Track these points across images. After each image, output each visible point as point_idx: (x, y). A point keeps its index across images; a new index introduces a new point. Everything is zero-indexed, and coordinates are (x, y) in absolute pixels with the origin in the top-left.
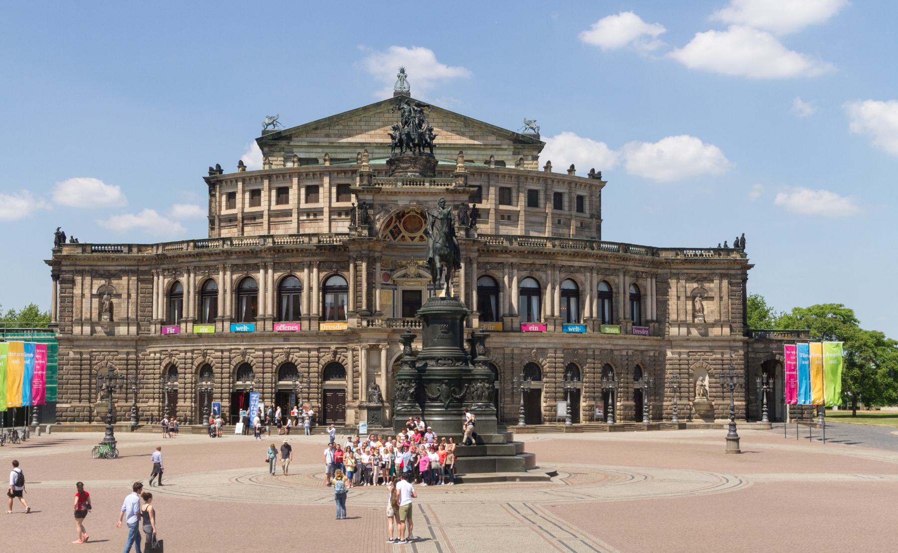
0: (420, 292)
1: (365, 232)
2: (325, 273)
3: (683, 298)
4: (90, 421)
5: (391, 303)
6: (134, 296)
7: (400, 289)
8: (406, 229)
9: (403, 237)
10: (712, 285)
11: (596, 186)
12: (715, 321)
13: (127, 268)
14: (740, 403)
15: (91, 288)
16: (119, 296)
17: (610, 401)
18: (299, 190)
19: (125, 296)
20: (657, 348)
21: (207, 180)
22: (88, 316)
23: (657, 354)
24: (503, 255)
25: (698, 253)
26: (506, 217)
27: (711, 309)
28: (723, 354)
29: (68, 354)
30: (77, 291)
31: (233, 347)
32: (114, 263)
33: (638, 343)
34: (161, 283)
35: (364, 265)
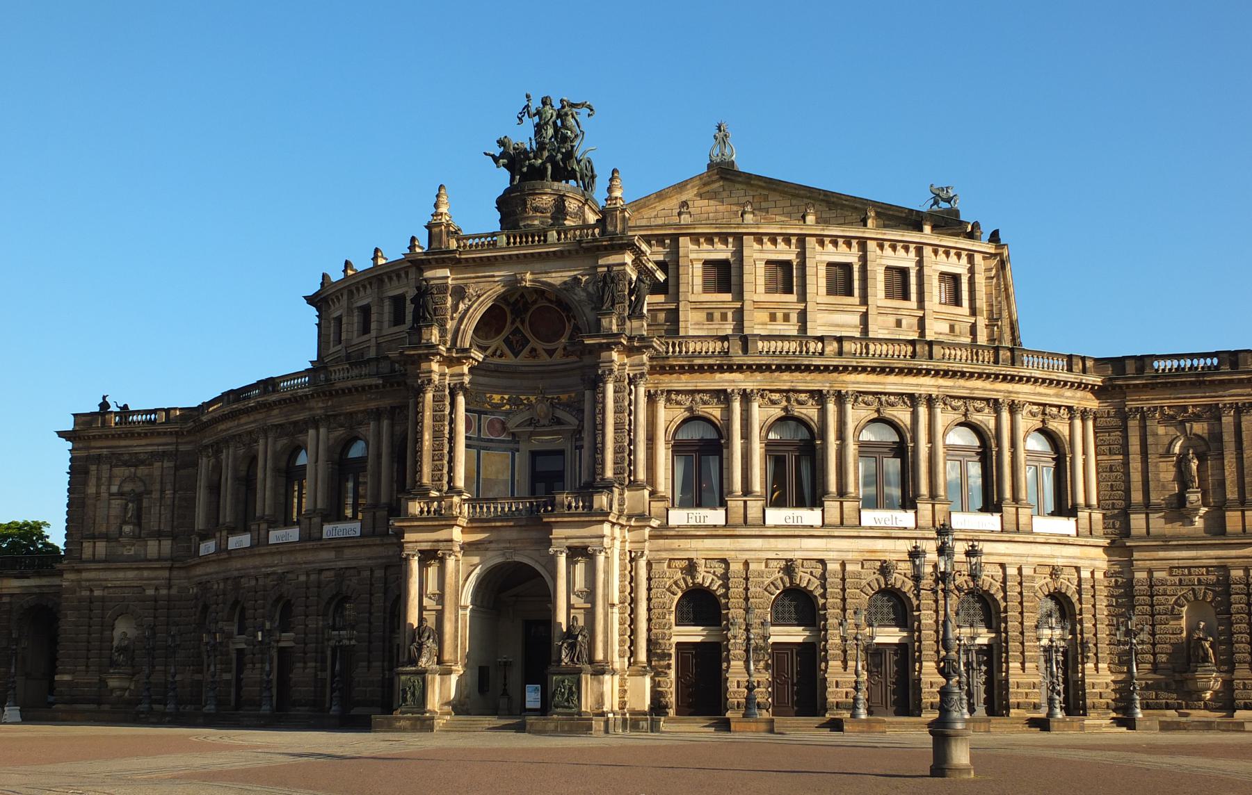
0: (561, 453)
4: (99, 704)
5: (507, 476)
7: (525, 448)
8: (537, 335)
9: (533, 350)
15: (110, 485)
19: (156, 495)
21: (311, 300)
23: (1099, 575)
24: (727, 376)
26: (780, 315)
29: (75, 592)
30: (92, 490)
31: (269, 570)
32: (143, 442)
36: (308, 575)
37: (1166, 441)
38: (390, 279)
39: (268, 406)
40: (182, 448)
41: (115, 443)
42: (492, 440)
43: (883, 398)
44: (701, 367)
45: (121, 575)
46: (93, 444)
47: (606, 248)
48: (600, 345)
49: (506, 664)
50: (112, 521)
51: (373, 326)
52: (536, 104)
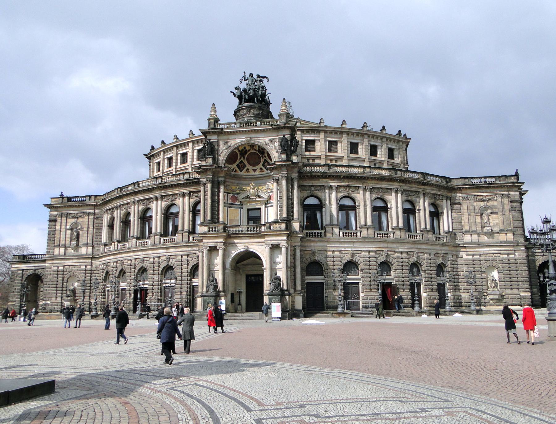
0: (260, 209)
1: (210, 161)
2: (194, 199)
3: (473, 214)
6: (91, 228)
9: (248, 169)
10: (495, 203)
11: (403, 142)
12: (500, 230)
13: (88, 211)
14: (526, 294)
15: (66, 225)
16: (82, 228)
17: (416, 291)
18: (193, 152)
19: (86, 229)
20: (454, 253)
22: (64, 243)
24: (324, 180)
25: (483, 180)
27: (496, 221)
28: (508, 255)
30: (58, 227)
31: (137, 257)
32: (80, 208)
33: (438, 248)
34: (106, 218)
35: (209, 186)
36: (154, 258)
37: (477, 208)
38: (181, 146)
39: (136, 193)
40: (97, 211)
41: (69, 209)
42: (232, 204)
43: (381, 190)
44: (315, 176)
45: (71, 261)
46: (59, 209)
47: (282, 128)
48: (282, 165)
49: (240, 292)
50: (67, 239)
51: (174, 164)
52: (247, 76)
